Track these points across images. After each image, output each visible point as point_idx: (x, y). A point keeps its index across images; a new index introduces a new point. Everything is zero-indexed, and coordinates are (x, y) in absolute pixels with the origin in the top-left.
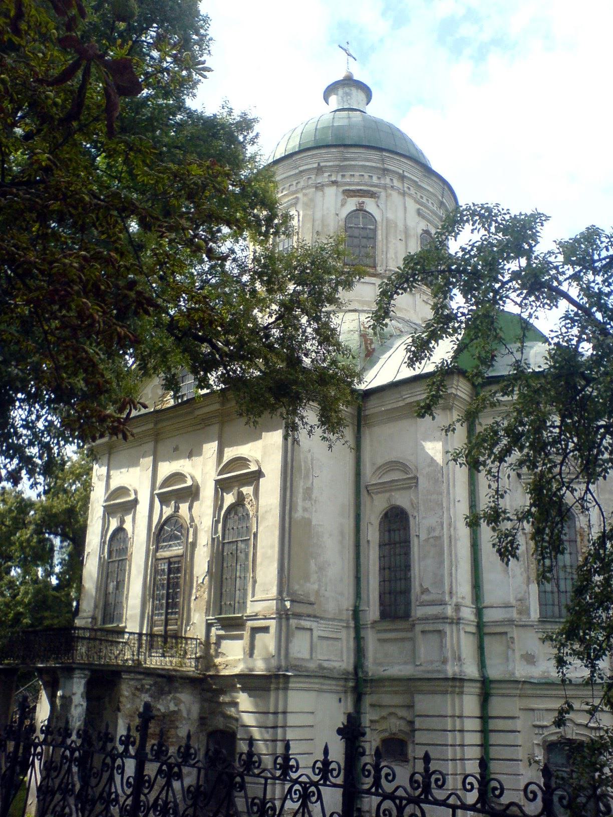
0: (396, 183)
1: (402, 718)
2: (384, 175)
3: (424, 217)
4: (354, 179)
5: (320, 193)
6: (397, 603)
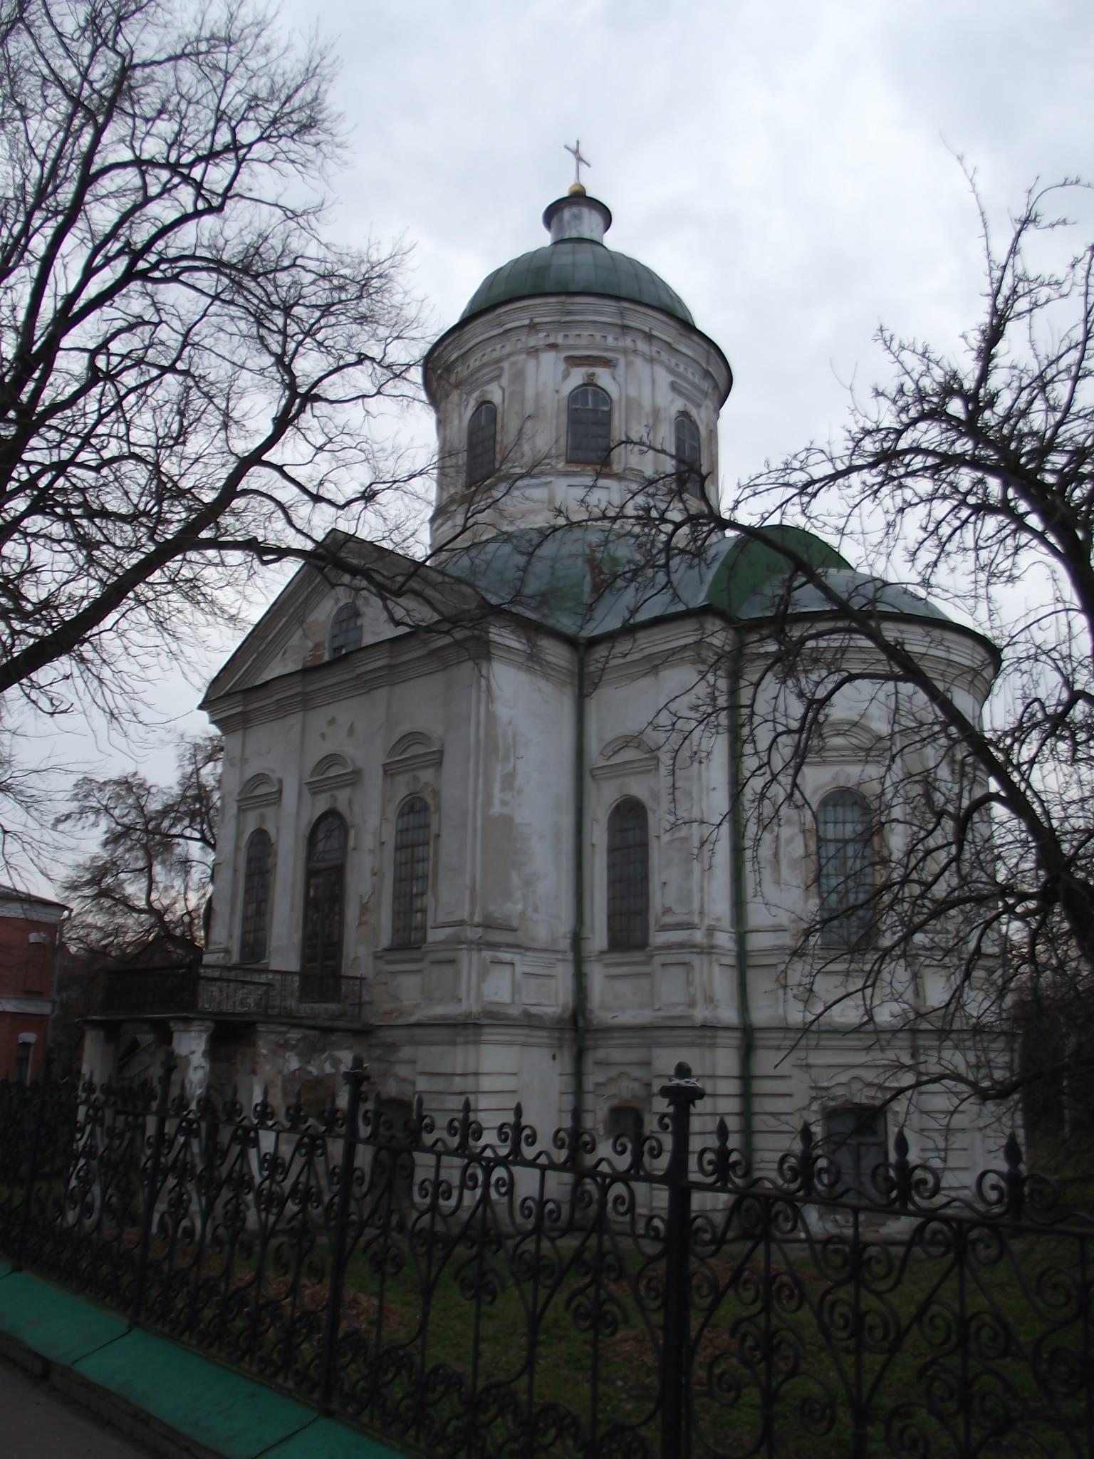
0: (642, 345)
1: (636, 1080)
2: (624, 334)
4: (582, 341)
5: (531, 363)
6: (630, 931)
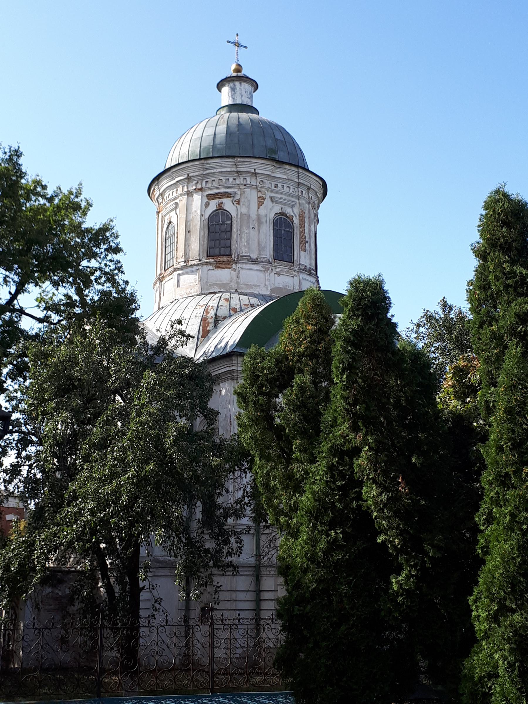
3: (277, 202)
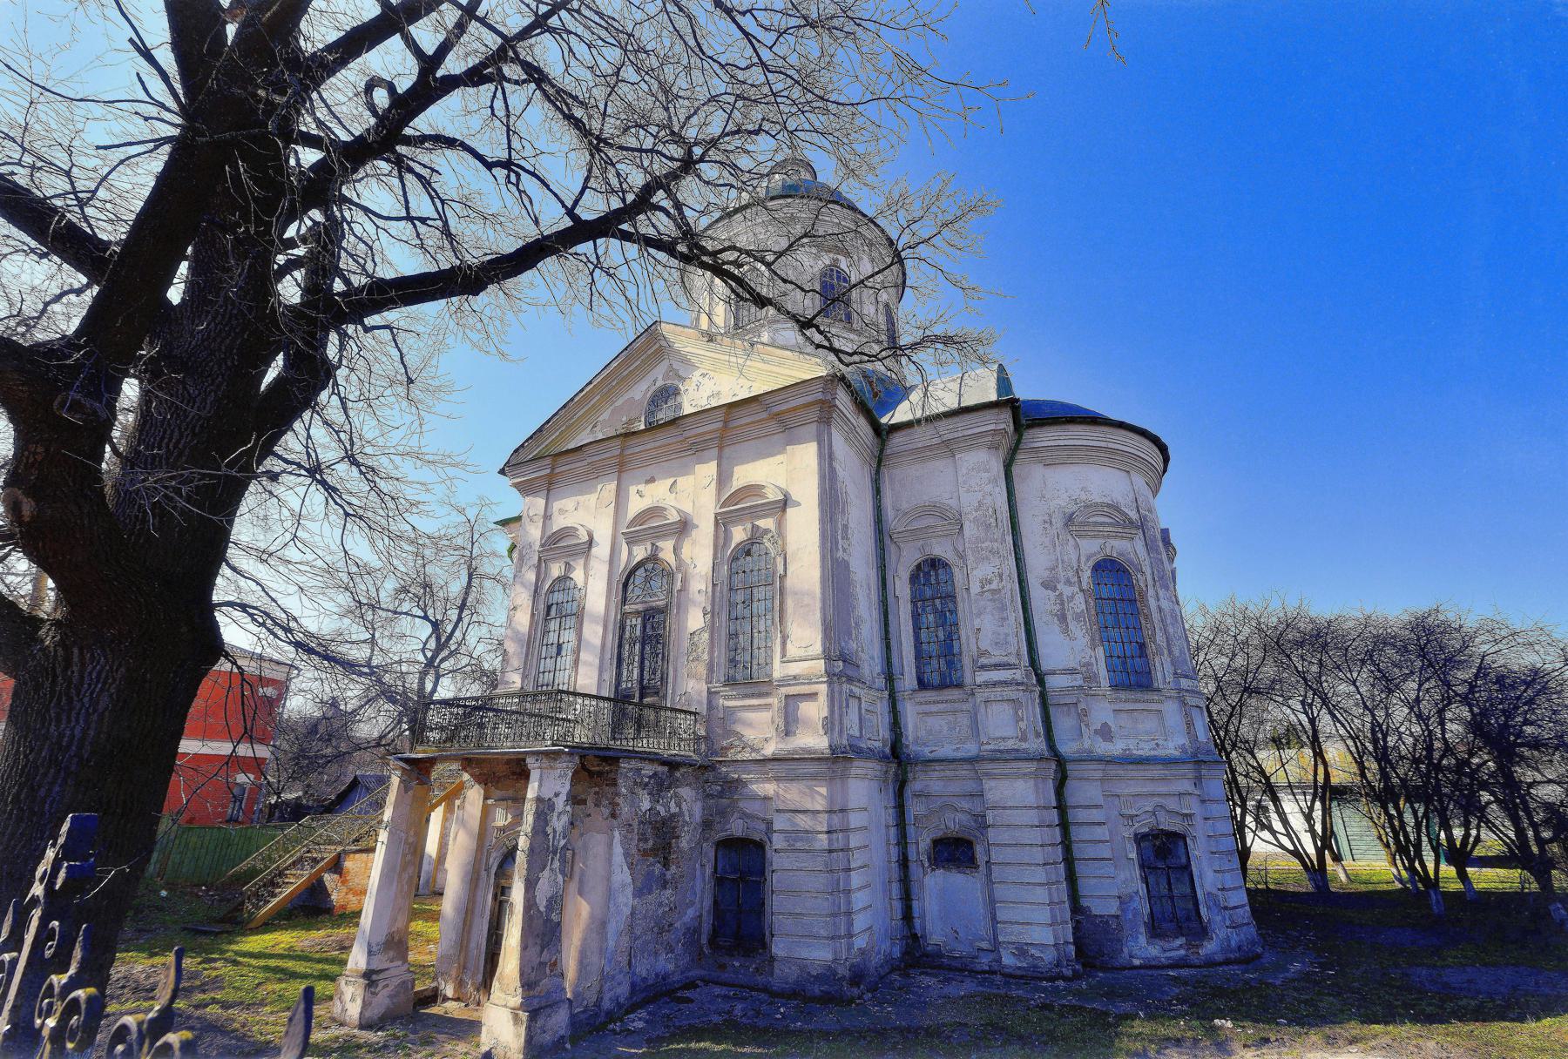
6: (942, 670)
